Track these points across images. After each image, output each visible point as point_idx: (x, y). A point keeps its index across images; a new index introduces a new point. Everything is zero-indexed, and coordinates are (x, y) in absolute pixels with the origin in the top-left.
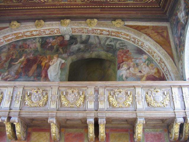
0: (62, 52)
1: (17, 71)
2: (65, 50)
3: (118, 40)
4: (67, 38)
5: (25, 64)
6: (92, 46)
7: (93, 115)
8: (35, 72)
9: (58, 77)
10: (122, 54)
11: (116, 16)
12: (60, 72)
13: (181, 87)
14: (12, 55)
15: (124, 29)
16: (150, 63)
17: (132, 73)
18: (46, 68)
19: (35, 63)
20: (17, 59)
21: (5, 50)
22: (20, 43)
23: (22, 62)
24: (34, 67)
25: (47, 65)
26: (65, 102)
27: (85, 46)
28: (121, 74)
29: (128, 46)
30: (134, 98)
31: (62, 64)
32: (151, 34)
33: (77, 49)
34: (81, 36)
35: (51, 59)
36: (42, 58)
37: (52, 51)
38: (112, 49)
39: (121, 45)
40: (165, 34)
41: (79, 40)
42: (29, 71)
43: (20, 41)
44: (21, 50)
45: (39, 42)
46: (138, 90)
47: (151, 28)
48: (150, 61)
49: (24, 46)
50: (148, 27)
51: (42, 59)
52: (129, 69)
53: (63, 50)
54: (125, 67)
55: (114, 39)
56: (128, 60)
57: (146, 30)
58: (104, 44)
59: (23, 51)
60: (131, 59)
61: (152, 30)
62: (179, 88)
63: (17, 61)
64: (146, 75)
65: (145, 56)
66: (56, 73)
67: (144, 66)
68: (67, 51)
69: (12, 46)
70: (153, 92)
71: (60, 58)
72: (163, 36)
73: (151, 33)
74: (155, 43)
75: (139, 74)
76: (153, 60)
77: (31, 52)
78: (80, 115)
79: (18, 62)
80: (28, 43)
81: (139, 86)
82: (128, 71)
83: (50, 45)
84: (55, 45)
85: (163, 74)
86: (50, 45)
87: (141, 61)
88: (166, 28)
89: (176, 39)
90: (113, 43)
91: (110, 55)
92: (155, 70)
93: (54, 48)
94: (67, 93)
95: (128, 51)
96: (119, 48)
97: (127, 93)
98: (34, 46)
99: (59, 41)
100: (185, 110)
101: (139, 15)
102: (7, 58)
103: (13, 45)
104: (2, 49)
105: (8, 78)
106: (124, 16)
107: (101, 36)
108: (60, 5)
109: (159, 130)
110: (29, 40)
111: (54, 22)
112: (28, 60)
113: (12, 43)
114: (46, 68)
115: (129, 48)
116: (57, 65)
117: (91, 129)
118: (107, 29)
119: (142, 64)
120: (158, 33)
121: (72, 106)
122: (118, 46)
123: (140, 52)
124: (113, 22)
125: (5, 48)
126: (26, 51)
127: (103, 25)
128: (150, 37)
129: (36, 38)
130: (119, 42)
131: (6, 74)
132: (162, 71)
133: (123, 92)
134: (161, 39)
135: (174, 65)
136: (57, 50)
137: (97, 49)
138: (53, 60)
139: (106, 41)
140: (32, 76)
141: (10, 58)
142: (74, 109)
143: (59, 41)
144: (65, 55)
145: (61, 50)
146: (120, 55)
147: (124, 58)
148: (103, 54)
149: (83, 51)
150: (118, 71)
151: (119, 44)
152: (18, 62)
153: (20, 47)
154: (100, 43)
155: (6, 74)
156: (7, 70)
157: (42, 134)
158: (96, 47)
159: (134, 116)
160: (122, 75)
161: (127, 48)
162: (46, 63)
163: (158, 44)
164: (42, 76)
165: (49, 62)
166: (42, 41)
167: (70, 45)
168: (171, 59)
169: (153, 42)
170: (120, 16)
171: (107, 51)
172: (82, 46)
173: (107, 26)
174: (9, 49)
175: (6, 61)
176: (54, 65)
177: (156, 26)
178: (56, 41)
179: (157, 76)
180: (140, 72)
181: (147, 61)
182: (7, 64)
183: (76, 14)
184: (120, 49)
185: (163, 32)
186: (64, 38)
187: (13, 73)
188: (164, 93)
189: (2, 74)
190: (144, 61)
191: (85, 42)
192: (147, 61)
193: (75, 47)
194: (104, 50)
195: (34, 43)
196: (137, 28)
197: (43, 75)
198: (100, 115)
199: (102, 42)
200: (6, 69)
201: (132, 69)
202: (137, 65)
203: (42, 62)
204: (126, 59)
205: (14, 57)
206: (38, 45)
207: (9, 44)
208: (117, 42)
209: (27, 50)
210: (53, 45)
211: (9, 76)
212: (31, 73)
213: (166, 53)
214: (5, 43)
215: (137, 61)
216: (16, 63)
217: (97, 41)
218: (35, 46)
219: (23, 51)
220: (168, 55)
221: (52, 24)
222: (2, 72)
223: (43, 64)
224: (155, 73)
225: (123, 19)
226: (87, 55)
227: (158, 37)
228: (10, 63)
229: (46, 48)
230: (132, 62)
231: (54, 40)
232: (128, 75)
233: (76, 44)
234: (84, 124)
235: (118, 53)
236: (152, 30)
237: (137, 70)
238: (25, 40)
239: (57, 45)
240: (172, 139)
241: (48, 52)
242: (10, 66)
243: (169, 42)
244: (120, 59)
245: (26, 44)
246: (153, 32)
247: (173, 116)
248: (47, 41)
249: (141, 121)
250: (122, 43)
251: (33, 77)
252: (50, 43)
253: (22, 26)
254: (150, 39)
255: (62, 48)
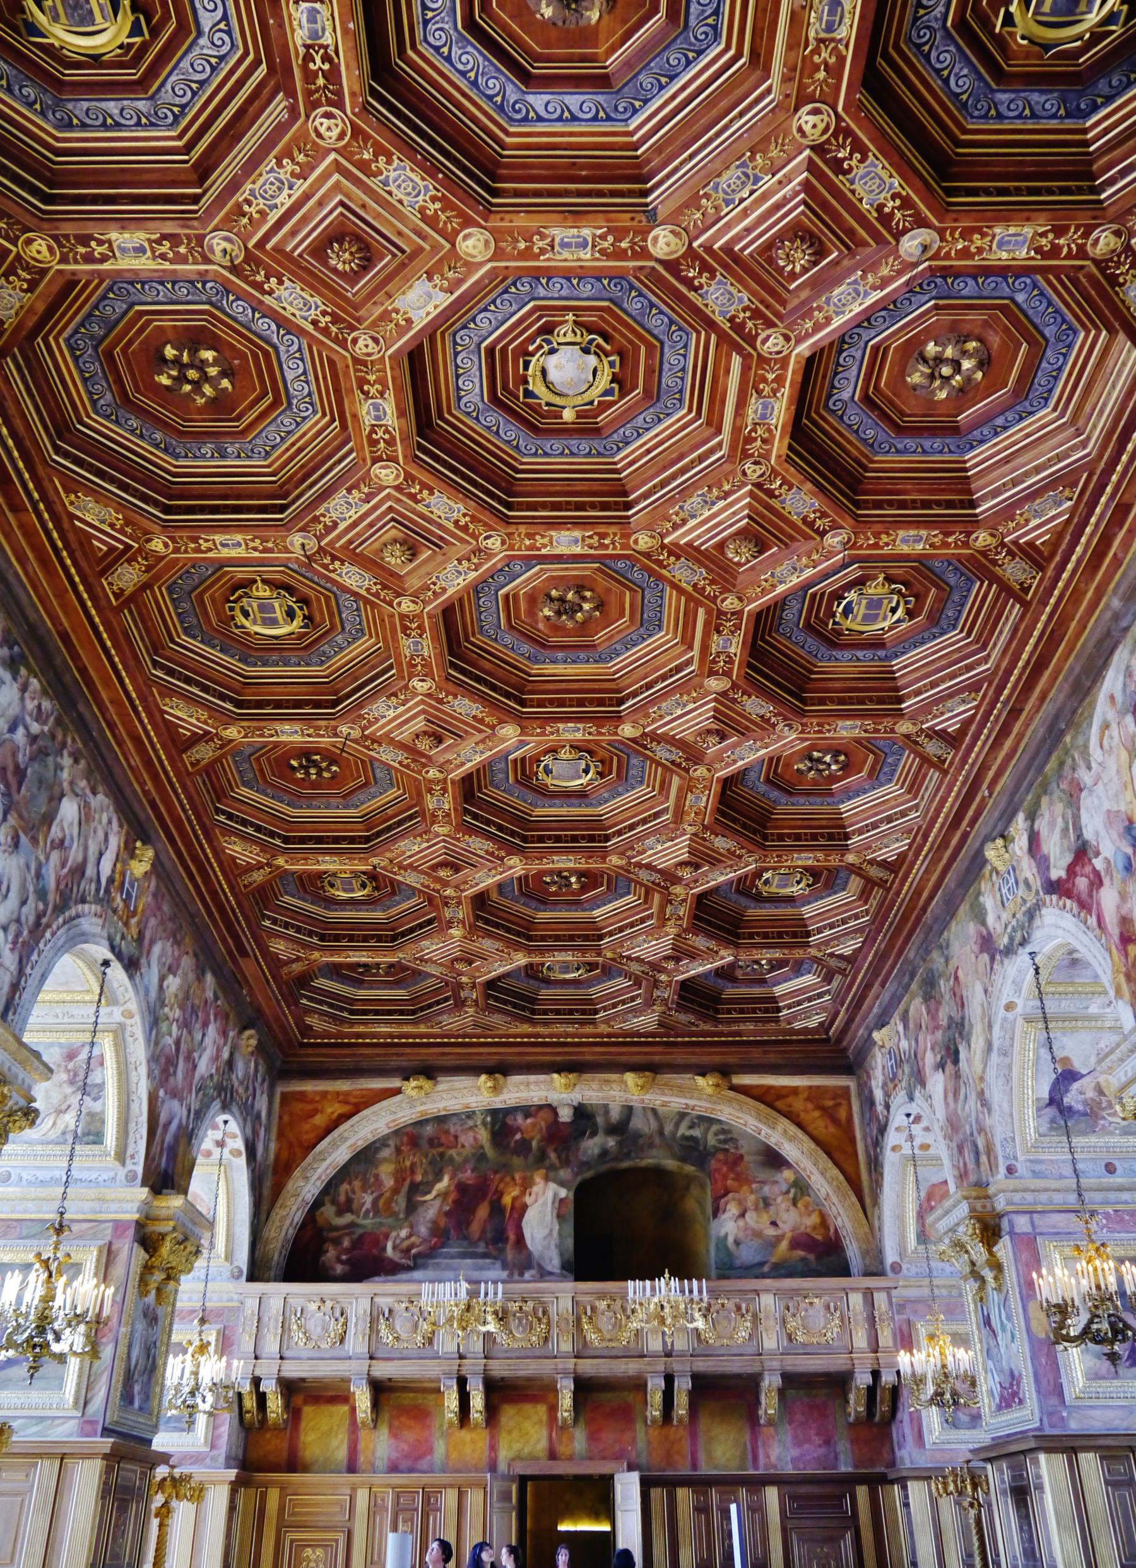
0: (557, 1162)
1: (435, 1222)
2: (563, 1156)
3: (711, 1121)
4: (565, 1115)
5: (454, 1202)
6: (641, 1141)
7: (661, 1368)
8: (489, 1228)
9: (553, 1243)
10: (725, 1169)
11: (706, 1060)
12: (557, 1227)
13: (869, 1295)
14: (413, 1172)
15: (730, 1101)
16: (802, 1195)
17: (753, 1230)
18: (516, 1215)
19: (484, 1197)
20: (429, 1186)
21: (386, 1153)
22: (429, 1130)
23: (444, 1195)
24: (483, 1211)
25: (517, 1204)
26: (592, 1337)
27: (620, 1144)
28: (722, 1233)
29: (741, 1143)
30: (756, 1320)
31: (562, 1201)
32: (802, 1115)
33: (597, 1151)
34: (606, 1106)
35: (527, 1185)
36: (501, 1180)
37: (526, 1157)
38: (696, 1154)
39: (722, 1137)
40: (842, 1114)
41: (600, 1120)
42: (468, 1223)
43: (427, 1121)
44: (435, 1151)
45: (484, 1124)
46: (767, 1301)
47: (805, 1095)
48: (801, 1187)
49: (443, 1140)
50: (795, 1091)
51: (501, 1186)
52: (742, 1215)
53: (559, 1157)
54: (733, 1209)
55: (700, 1118)
56: (741, 1186)
57: (790, 1100)
58: (674, 1134)
59: (442, 1155)
60: (748, 1182)
61: (808, 1099)
62: (865, 1294)
63: (429, 1192)
64: (789, 1235)
65: (787, 1174)
66: (546, 1231)
67: (783, 1206)
68: (572, 1158)
69: (405, 1139)
70: (803, 1305)
71: (555, 1181)
72: (835, 1121)
73: (806, 1111)
74: (813, 1146)
75: (771, 1232)
76: (808, 1186)
77: (466, 1160)
78: (630, 1368)
79: (434, 1193)
80: (452, 1130)
81: (767, 1291)
82: (741, 1223)
83: (518, 1136)
84: (532, 1139)
85: (836, 1231)
86: (518, 1136)
87: (776, 1189)
88: (848, 1088)
89: (869, 1140)
90: (696, 1133)
91: (689, 1169)
92: (814, 1219)
93: (530, 1148)
94: (593, 1309)
95: (741, 1157)
96: (714, 1147)
97: (739, 1308)
98: (471, 1140)
99: (542, 1120)
100: (876, 1352)
101: (772, 1058)
102: (400, 1176)
103: (407, 1134)
104: (378, 1150)
105: (412, 1246)
106: (732, 1059)
107: (660, 1110)
108: (551, 1036)
109: (823, 1392)
110: (455, 1120)
111: (533, 1078)
112: (462, 1188)
113: (409, 1129)
114: (516, 1215)
115: (745, 1148)
116: (545, 1204)
117: (656, 1398)
118: (683, 1101)
119: (779, 1199)
120: (822, 1108)
121: (611, 1344)
122: (712, 1141)
123: (774, 1160)
124: (700, 1081)
125: (388, 1146)
126: (451, 1158)
127: (671, 1087)
128: (800, 1125)
129: (474, 1112)
130: (714, 1128)
131: (404, 1233)
132: (831, 1222)
133: (730, 1305)
134: (832, 1129)
135: (861, 1214)
136: (542, 1156)
137: (654, 1152)
138: (535, 1189)
139: (677, 1125)
140: (479, 1239)
141: (408, 1181)
142: (613, 1353)
143: (543, 1123)
144: (565, 1174)
145: (553, 1156)
146: (719, 1170)
147: (729, 1182)
148: (670, 1164)
149: (616, 1159)
150: (714, 1224)
151: (716, 1134)
152: (434, 1193)
153: (432, 1142)
154: (661, 1132)
155: (404, 1233)
156: (407, 1218)
157: (528, 1408)
158: (651, 1145)
159: (755, 1368)
160: (726, 1236)
161: (737, 1148)
162: (514, 1199)
163: (820, 1152)
164: (506, 1240)
165: (523, 1193)
166: (493, 1123)
167: (576, 1138)
168: (854, 1199)
169: (809, 1144)
170: (717, 1059)
171: (683, 1160)
172: (611, 1142)
173: (681, 1090)
174: (398, 1150)
175: (396, 1191)
176: (540, 1202)
177: (818, 1087)
178: (534, 1125)
179: (819, 1238)
180: (774, 1224)
181: (793, 1191)
182: (401, 1203)
183: (593, 1054)
184: (717, 1150)
185: (838, 1105)
186: (556, 1114)
187: (423, 1230)
188: (828, 1307)
189: (394, 1234)
190: (784, 1189)
191: (620, 1129)
192: (793, 1191)
193: (592, 1146)
194: (674, 1156)
195: (471, 1128)
196: (765, 1098)
197: (512, 1237)
198: (676, 1366)
199: (668, 1129)
200: (402, 1216)
201: (750, 1216)
202: (767, 1203)
203: (501, 1194)
204: (735, 1184)
205: (419, 1178)
206: (483, 1135)
207: (397, 1133)
208: (708, 1130)
209: (453, 1152)
210: (527, 1136)
211: (413, 1239)
212: (475, 1228)
213: (841, 1178)
214: (387, 1131)
215: (766, 1189)
216: (428, 1197)
217: (654, 1124)
218: (475, 1139)
219: (442, 1155)
220: (845, 1184)
221: (528, 1084)
222: (392, 1228)
223: (507, 1200)
224: (814, 1228)
225: (725, 1071)
226: (625, 1164)
227: (821, 1126)
228: (409, 1199)
229: (508, 1146)
230: (752, 1192)
231: (529, 1121)
232: (741, 1235)
233: (594, 1134)
234: (639, 1385)
235: (713, 1164)
236: (808, 1099)
237: (765, 1219)
238: (441, 1120)
239: (538, 1137)
240: (852, 1419)
241: (517, 1161)
242: (412, 1207)
243: (853, 1140)
244: (720, 1184)
245: (447, 1132)
246: (810, 1106)
247: (848, 1367)
248: (509, 1121)
249: (771, 1382)
250: (724, 1132)
251: (482, 1245)
252: (519, 1129)
253: (440, 1087)
254: (800, 1133)
255: (555, 1150)
